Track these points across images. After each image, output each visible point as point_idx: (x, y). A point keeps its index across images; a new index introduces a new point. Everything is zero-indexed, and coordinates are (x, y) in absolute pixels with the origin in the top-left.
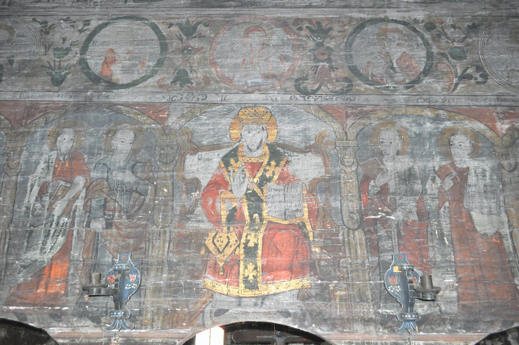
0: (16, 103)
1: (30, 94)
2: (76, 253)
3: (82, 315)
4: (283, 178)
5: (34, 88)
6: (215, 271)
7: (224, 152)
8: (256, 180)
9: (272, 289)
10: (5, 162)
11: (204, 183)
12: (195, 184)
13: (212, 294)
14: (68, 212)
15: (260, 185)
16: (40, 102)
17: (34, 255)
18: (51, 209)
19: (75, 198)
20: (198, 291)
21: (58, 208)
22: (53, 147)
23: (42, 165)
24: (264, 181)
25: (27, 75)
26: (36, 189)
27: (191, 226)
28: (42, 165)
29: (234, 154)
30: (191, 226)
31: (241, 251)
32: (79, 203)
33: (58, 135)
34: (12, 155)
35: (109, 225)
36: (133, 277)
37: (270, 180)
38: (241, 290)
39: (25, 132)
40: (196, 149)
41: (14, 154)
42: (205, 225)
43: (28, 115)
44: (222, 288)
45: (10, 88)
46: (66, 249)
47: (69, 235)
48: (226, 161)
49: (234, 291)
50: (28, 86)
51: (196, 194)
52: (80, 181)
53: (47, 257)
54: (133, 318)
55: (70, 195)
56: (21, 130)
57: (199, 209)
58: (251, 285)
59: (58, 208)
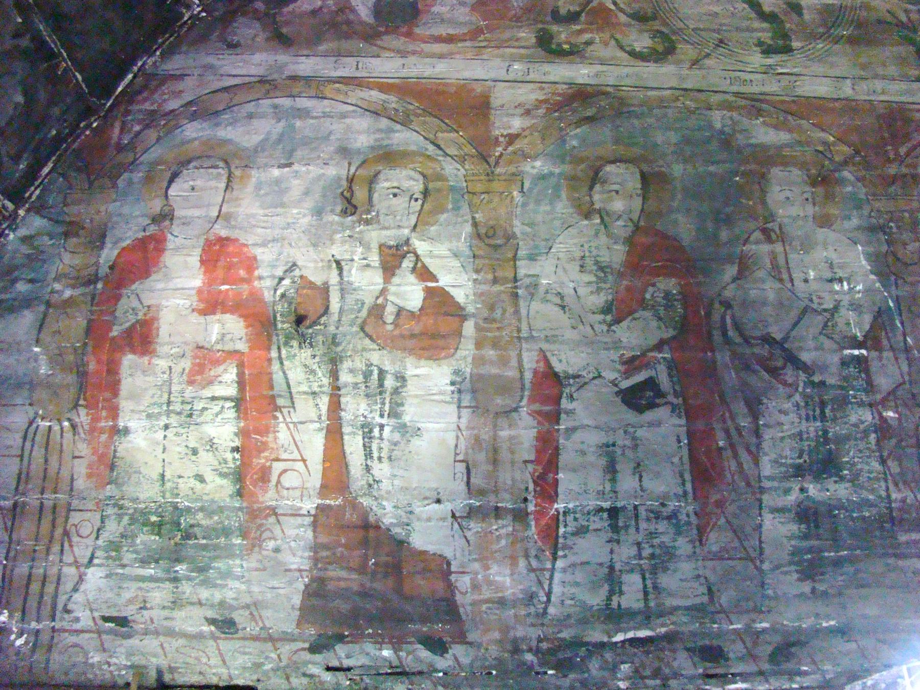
0: (850, 107)
1: (878, 85)
5: (880, 71)
10: (884, 248)
16: (908, 106)
25: (852, 41)
34: (894, 230)
39: (905, 176)
41: (898, 228)
43: (893, 136)
45: (819, 69)
50: (864, 67)
56: (892, 170)
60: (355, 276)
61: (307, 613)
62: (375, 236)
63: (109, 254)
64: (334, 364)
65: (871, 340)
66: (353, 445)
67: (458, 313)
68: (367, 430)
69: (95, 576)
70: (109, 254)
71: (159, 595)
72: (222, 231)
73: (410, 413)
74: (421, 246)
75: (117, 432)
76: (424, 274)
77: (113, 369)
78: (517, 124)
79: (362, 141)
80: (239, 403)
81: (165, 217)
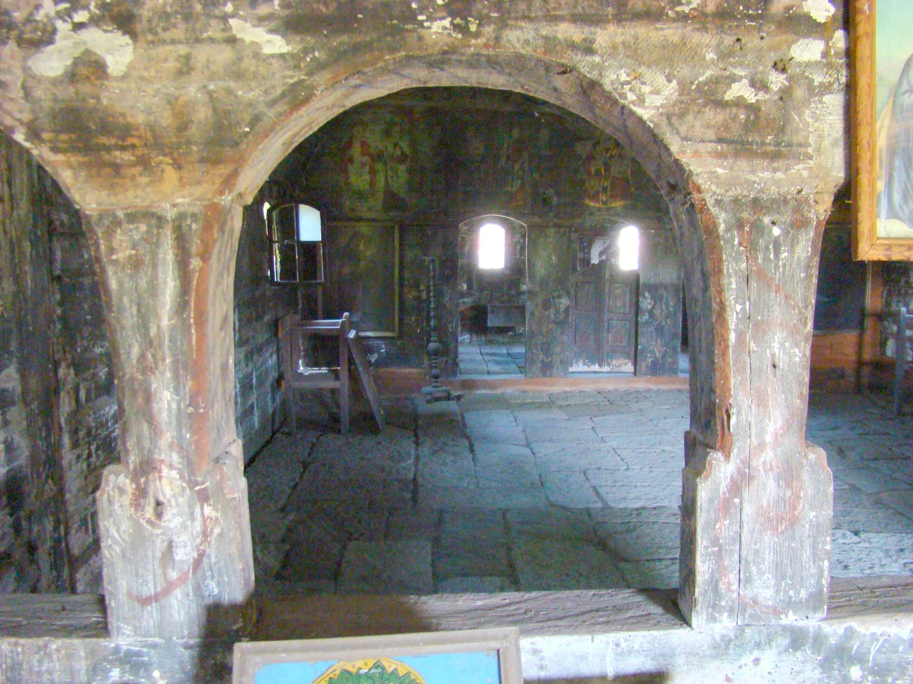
2: (528, 188)
3: (534, 214)
4: (620, 155)
6: (589, 197)
7: (593, 142)
8: (608, 156)
9: (614, 205)
11: (584, 157)
12: (579, 157)
13: (588, 206)
14: (522, 168)
15: (610, 158)
17: (509, 189)
18: (513, 167)
19: (524, 162)
20: (583, 205)
21: (517, 167)
22: (510, 136)
23: (506, 146)
24: (611, 157)
26: (505, 157)
27: (579, 176)
28: (506, 146)
29: (597, 143)
30: (579, 176)
31: (600, 189)
32: (526, 165)
33: (511, 131)
35: (541, 176)
36: (555, 199)
37: (614, 156)
38: (600, 205)
40: (579, 139)
42: (585, 177)
44: (592, 204)
46: (523, 186)
47: (523, 180)
48: (594, 146)
49: (597, 205)
51: (580, 162)
52: (526, 155)
53: (515, 189)
54: (556, 216)
55: (521, 161)
57: (582, 169)
58: (605, 203)
59: (517, 167)
60: (389, 149)
61: (383, 206)
62: (392, 140)
63: (343, 144)
64: (385, 164)
65: (481, 162)
66: (390, 180)
67: (406, 156)
68: (392, 177)
69: (348, 202)
70: (343, 144)
71: (359, 204)
72: (363, 139)
73: (400, 174)
74: (401, 143)
75: (348, 178)
76: (401, 149)
77: (346, 166)
78: (418, 116)
79: (388, 120)
80: (370, 172)
81: (351, 138)
